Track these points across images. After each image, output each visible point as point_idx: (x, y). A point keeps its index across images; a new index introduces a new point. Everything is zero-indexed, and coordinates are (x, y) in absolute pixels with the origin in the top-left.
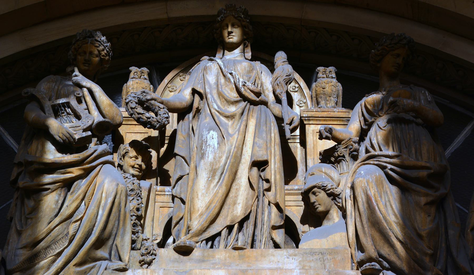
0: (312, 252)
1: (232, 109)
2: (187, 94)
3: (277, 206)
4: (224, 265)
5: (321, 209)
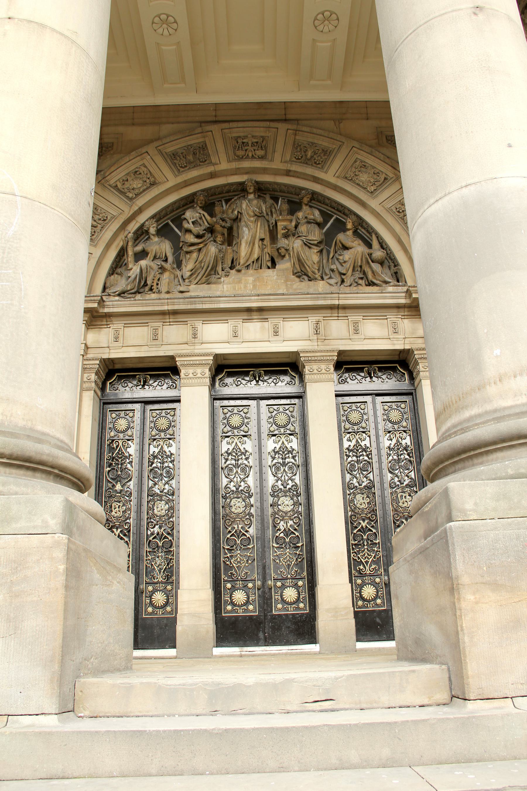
0: (280, 270)
1: (252, 219)
2: (236, 212)
3: (268, 253)
4: (252, 275)
5: (283, 254)
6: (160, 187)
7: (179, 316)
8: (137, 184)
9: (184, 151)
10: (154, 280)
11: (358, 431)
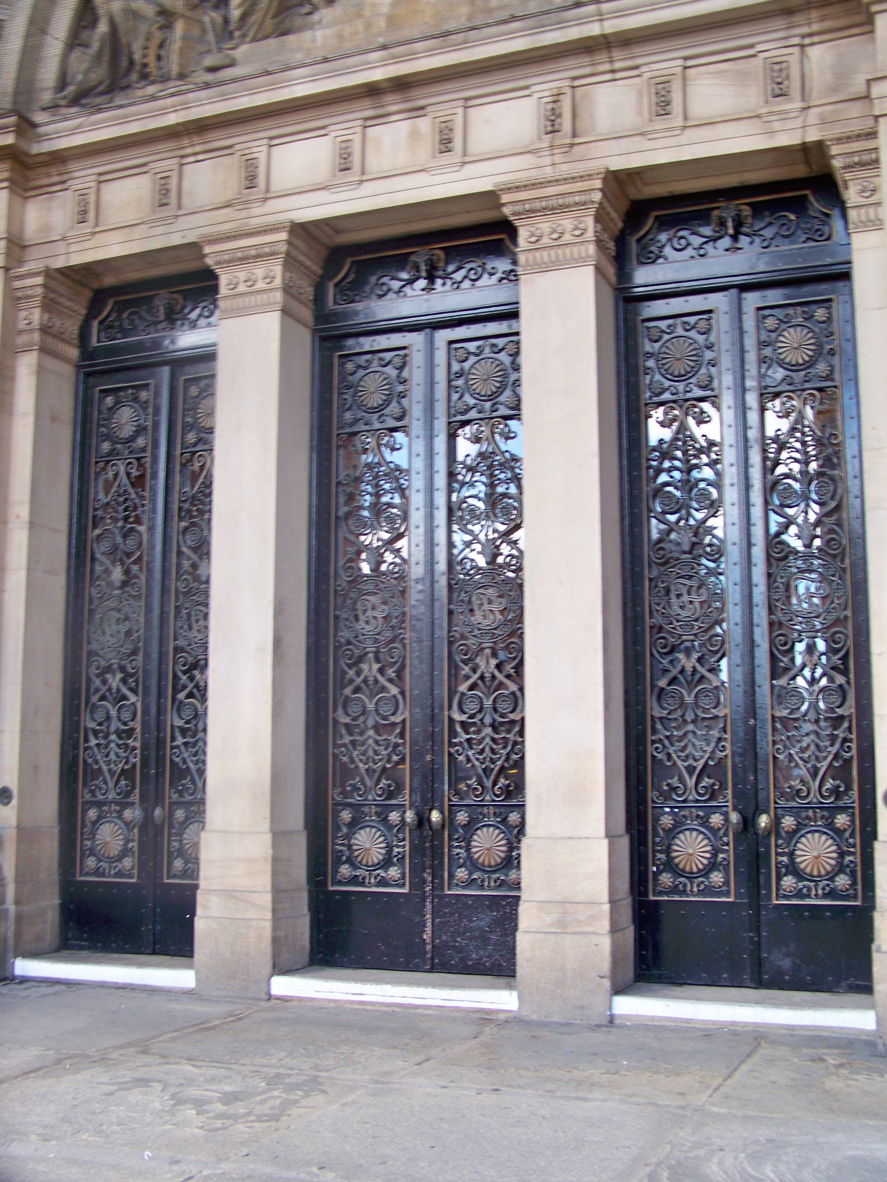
10: (146, 48)
11: (689, 395)
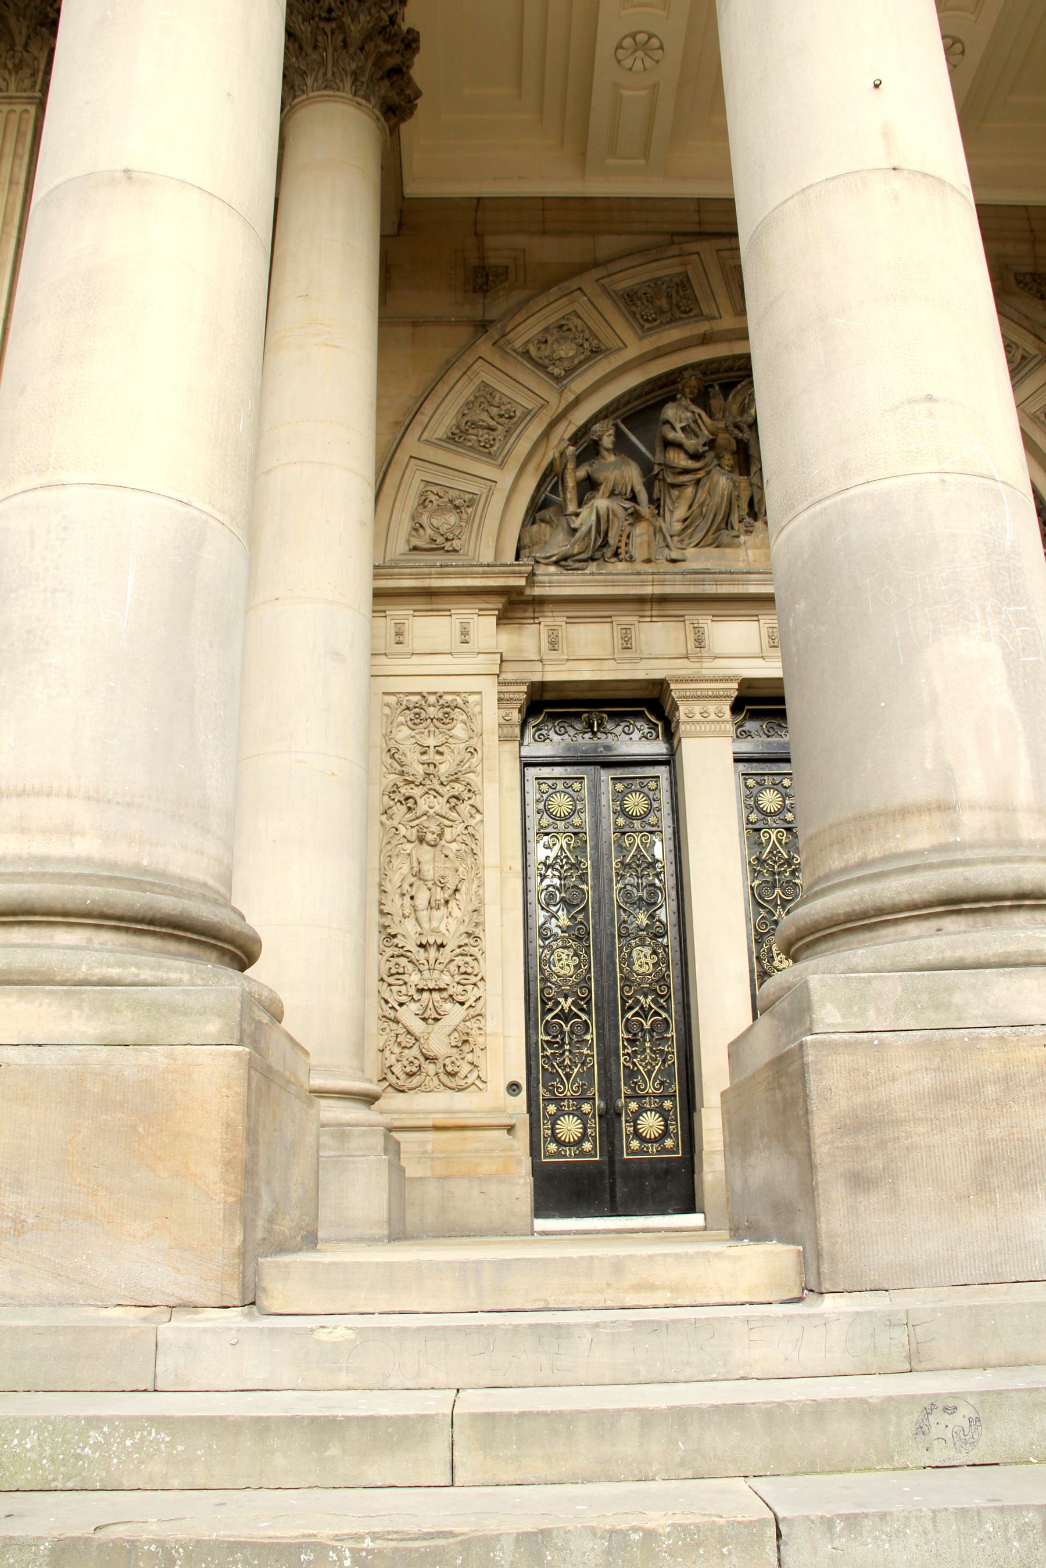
6: (612, 358)
7: (669, 606)
8: (566, 350)
9: (649, 290)
